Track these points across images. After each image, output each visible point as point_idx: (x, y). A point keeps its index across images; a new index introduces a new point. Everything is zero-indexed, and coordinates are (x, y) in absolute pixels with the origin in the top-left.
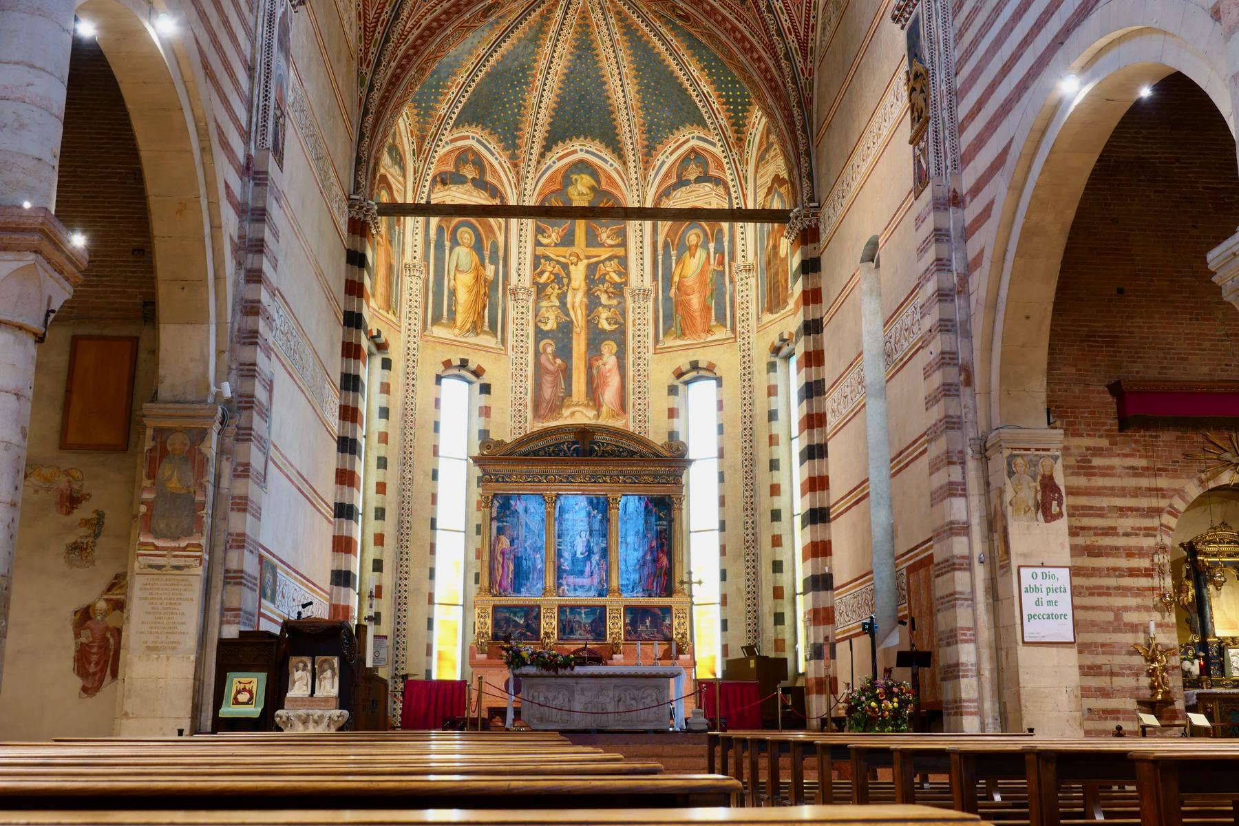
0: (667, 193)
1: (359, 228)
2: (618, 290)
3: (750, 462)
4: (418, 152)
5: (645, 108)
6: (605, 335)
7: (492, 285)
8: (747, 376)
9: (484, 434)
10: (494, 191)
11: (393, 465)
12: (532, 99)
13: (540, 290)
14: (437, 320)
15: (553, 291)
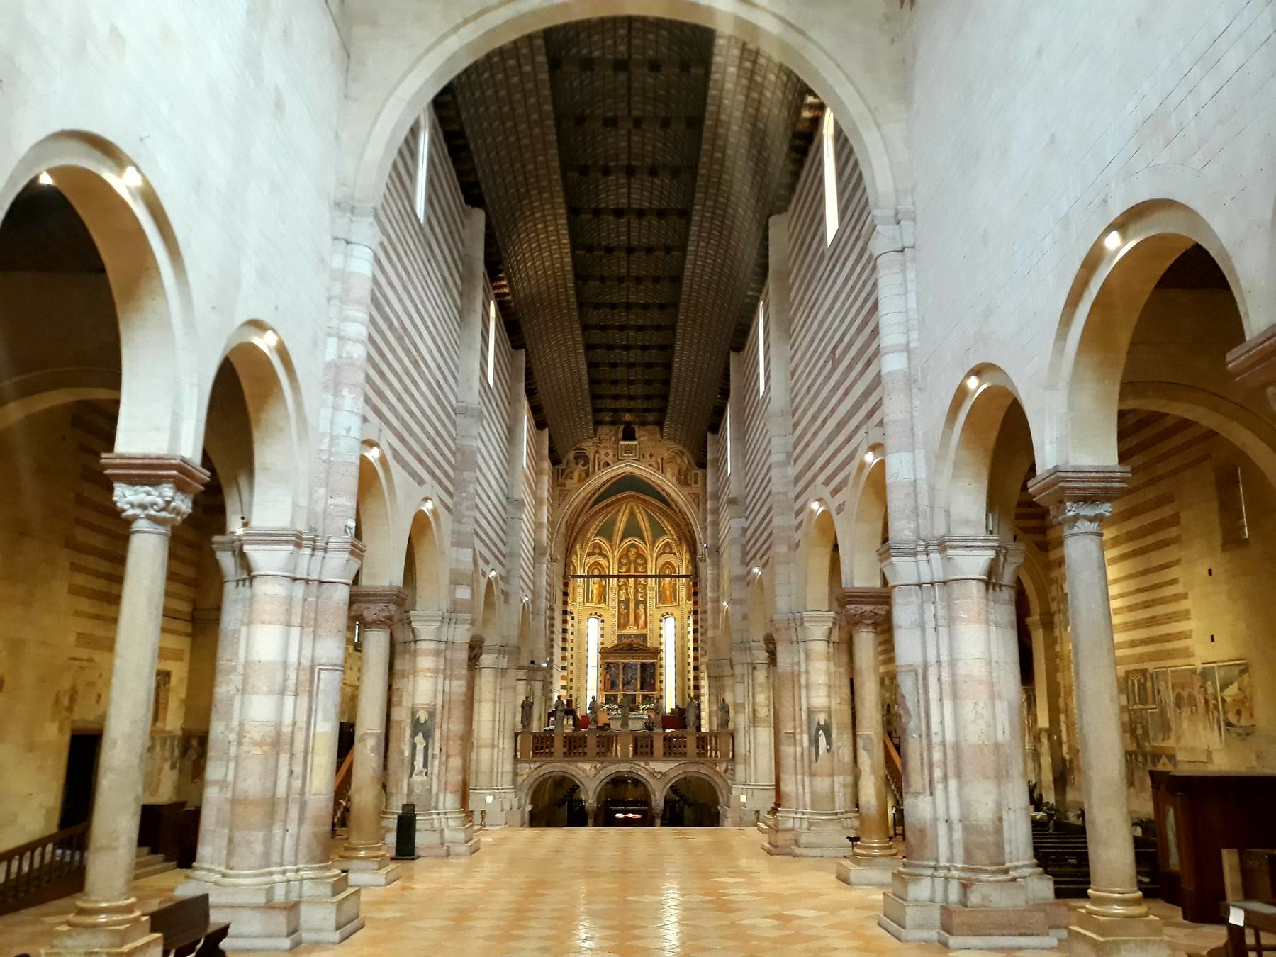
0: (659, 556)
1: (566, 585)
2: (644, 587)
3: (683, 646)
4: (581, 548)
5: (652, 530)
6: (641, 602)
7: (605, 587)
8: (682, 619)
9: (602, 643)
10: (605, 556)
11: (575, 649)
12: (617, 528)
13: (620, 587)
14: (587, 601)
15: (624, 587)
